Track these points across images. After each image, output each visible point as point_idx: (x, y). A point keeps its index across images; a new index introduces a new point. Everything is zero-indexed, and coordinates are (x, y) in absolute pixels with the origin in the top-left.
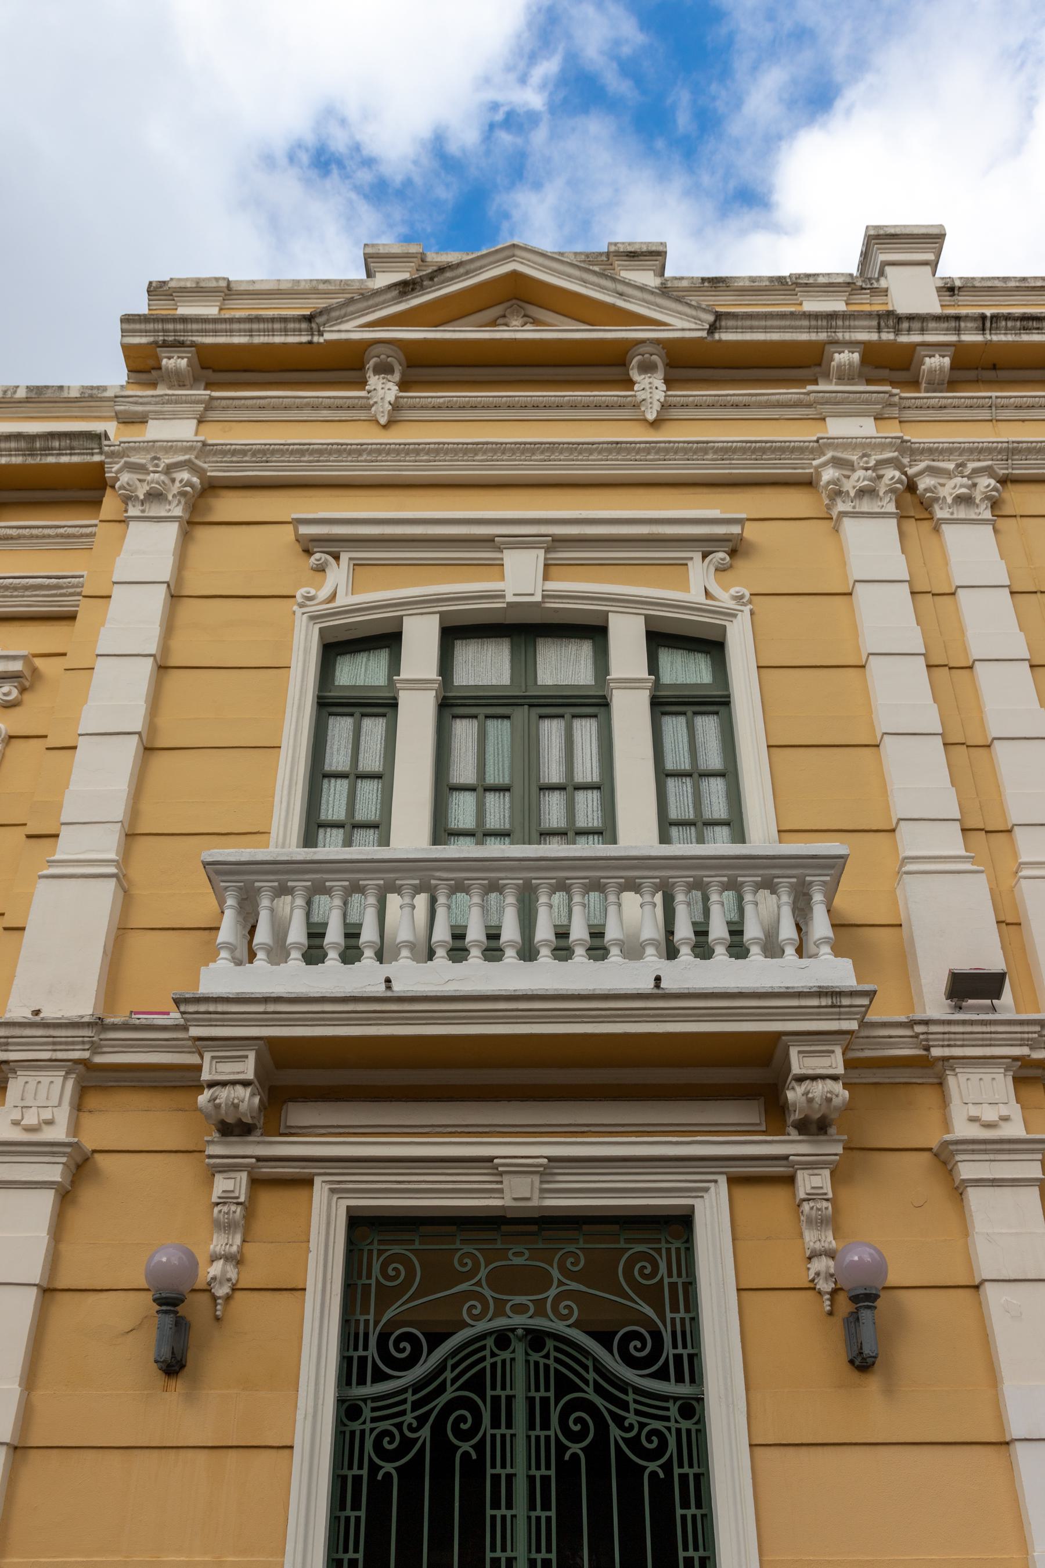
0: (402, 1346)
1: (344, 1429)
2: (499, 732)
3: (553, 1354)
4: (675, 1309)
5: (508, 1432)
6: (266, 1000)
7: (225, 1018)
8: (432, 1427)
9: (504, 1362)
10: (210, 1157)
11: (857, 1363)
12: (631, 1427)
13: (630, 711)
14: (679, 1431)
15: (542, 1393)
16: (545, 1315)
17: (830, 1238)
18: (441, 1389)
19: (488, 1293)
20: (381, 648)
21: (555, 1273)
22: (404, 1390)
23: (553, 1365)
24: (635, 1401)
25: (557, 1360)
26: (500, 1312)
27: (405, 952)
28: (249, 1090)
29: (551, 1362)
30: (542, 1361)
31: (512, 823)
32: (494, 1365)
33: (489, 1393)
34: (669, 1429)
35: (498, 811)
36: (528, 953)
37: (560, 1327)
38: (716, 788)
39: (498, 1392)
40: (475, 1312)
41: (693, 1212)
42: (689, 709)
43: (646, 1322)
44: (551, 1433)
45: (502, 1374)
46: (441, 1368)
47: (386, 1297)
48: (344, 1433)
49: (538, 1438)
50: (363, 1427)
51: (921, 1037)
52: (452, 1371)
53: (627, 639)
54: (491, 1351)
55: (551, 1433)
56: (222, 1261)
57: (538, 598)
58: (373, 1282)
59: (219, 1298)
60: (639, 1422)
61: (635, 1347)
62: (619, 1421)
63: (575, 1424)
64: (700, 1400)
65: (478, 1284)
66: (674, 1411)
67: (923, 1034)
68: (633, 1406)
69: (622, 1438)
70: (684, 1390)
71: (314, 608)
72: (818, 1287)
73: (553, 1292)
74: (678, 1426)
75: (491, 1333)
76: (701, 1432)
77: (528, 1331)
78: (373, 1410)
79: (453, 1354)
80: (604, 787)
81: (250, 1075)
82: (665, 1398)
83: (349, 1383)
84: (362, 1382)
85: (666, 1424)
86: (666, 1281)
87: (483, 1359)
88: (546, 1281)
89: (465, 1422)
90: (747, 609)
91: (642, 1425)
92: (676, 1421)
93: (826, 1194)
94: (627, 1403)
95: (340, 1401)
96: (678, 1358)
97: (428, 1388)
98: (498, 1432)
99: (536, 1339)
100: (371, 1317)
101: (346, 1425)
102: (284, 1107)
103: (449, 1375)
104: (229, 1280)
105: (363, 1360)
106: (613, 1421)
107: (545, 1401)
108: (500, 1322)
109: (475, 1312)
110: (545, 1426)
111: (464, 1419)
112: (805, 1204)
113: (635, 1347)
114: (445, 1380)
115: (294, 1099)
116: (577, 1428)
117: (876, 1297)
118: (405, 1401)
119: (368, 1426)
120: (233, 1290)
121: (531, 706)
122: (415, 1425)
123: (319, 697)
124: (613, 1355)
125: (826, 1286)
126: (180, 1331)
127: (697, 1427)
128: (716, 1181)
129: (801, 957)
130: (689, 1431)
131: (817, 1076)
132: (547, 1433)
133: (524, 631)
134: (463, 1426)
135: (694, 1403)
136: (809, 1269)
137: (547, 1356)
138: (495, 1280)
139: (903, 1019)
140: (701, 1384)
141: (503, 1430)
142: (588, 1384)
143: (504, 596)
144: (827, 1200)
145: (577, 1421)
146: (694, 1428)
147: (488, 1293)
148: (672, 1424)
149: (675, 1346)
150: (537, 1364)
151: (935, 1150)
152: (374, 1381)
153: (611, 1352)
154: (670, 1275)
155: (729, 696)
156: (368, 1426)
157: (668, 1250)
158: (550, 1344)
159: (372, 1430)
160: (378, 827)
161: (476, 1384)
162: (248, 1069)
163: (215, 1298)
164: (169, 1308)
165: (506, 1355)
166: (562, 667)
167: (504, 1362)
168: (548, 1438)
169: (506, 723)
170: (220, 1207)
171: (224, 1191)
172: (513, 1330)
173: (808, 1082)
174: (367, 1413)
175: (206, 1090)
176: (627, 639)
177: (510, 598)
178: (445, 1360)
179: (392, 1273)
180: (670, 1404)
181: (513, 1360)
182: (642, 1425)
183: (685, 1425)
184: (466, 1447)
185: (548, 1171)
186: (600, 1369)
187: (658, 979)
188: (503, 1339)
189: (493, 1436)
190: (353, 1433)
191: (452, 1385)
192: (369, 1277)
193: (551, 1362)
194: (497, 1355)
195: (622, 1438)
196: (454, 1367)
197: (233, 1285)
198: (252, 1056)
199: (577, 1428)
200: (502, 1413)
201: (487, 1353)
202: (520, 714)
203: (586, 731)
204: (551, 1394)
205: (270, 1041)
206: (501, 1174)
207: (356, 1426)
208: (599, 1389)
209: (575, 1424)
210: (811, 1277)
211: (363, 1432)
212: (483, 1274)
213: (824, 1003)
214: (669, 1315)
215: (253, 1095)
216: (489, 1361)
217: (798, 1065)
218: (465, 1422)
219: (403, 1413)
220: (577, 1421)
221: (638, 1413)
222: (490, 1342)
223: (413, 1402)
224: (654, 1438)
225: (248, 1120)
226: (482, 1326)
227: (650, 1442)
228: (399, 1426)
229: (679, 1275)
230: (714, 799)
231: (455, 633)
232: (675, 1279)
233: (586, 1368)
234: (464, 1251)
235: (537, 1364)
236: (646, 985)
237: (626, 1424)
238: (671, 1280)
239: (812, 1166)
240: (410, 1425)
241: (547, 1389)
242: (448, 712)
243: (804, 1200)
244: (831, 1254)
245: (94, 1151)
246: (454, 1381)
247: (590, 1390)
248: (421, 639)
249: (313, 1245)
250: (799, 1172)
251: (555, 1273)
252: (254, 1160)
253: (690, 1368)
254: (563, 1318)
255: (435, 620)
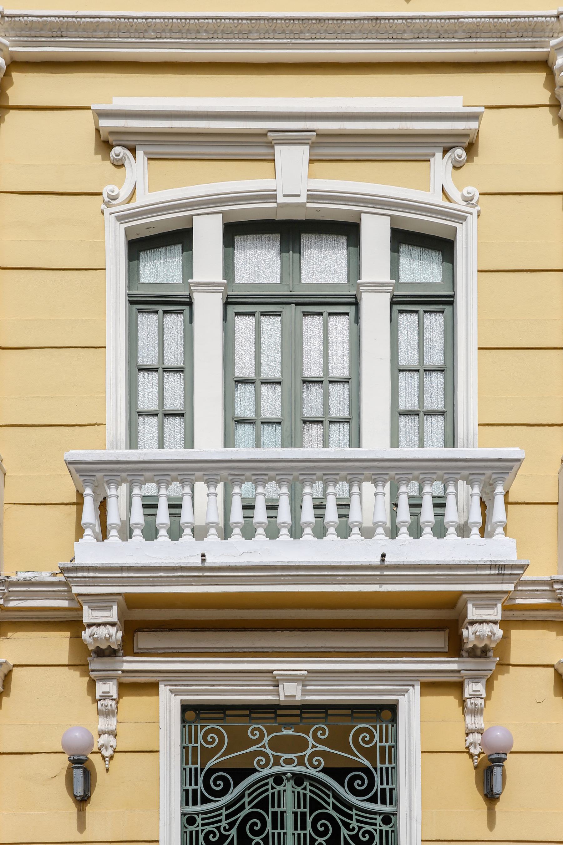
0: (218, 783)
1: (185, 830)
2: (272, 327)
3: (308, 787)
4: (383, 761)
5: (282, 832)
6: (122, 569)
7: (94, 582)
8: (238, 829)
9: (279, 792)
10: (93, 671)
11: (489, 796)
12: (354, 829)
13: (375, 307)
14: (381, 831)
15: (302, 810)
16: (304, 765)
17: (482, 722)
18: (242, 807)
19: (269, 751)
20: (175, 244)
21: (310, 740)
22: (221, 808)
23: (308, 794)
24: (357, 815)
25: (311, 791)
26: (277, 762)
27: (213, 531)
28: (115, 628)
29: (307, 792)
30: (302, 792)
31: (282, 414)
32: (273, 794)
33: (271, 810)
34: (376, 830)
35: (272, 402)
36: (296, 532)
37: (313, 772)
38: (436, 381)
39: (276, 809)
40: (261, 763)
41: (398, 703)
42: (421, 308)
43: (366, 770)
44: (307, 832)
45: (278, 798)
46: (242, 796)
47: (208, 754)
48: (186, 832)
49: (299, 834)
50: (197, 829)
51: (558, 591)
52: (248, 798)
53: (375, 233)
54: (272, 785)
55: (307, 832)
56: (106, 735)
57: (303, 199)
58: (198, 745)
59: (107, 757)
60: (358, 826)
61: (358, 784)
62: (347, 825)
63: (321, 827)
64: (395, 814)
65: (264, 746)
66: (379, 819)
67: (559, 589)
68: (355, 817)
69: (348, 835)
70: (386, 808)
71: (121, 208)
72: (471, 751)
73: (309, 751)
74: (381, 828)
75: (271, 776)
76: (395, 832)
77: (294, 774)
78: (203, 819)
79: (249, 788)
80: (352, 381)
81: (115, 619)
82: (375, 813)
83: (187, 804)
84: (195, 803)
85: (374, 827)
86: (379, 745)
87: (267, 790)
88: (304, 745)
89: (257, 826)
90: (474, 211)
91: (360, 828)
92: (380, 826)
93: (481, 695)
94: (352, 815)
95: (183, 815)
96: (383, 791)
97: (235, 807)
98: (276, 832)
99: (299, 779)
100: (199, 766)
101: (186, 828)
102: (136, 635)
103: (246, 799)
104: (112, 747)
105: (195, 792)
106: (343, 825)
107: (303, 814)
108: (277, 769)
109: (261, 763)
110: (304, 827)
111: (256, 824)
112: (468, 700)
113: (358, 784)
114: (244, 803)
115: (141, 630)
116: (322, 829)
117: (502, 760)
118: (221, 814)
119: (200, 828)
120: (115, 752)
121: (297, 304)
122: (227, 827)
123: (129, 296)
124: (344, 787)
125: (475, 751)
126: (82, 776)
127: (393, 829)
128: (413, 686)
129: (482, 536)
130: (387, 832)
131: (482, 623)
132: (305, 832)
133: (290, 232)
134: (256, 828)
135: (392, 816)
136: (466, 740)
137: (305, 789)
138: (273, 744)
139: (547, 578)
140: (397, 804)
141: (279, 830)
142: (329, 805)
143: (275, 197)
144: (482, 698)
145: (322, 825)
146: (390, 830)
147: (269, 751)
148: (377, 827)
149: (382, 784)
150: (299, 793)
151: (556, 667)
152: (202, 803)
153: (343, 786)
154: (381, 741)
155: (453, 296)
156: (200, 828)
157: (381, 727)
158: (306, 783)
159: (202, 830)
160: (183, 416)
161: (263, 804)
162: (113, 615)
163: (104, 758)
164: (79, 765)
165: (280, 788)
166: (323, 264)
167: (279, 792)
168: (305, 835)
169: (277, 320)
170: (102, 702)
171: (103, 693)
172: (285, 774)
173: (477, 624)
174: (199, 821)
175: (87, 630)
176: (375, 233)
177: (281, 200)
178: (245, 791)
179: (210, 740)
180: (377, 817)
181: (284, 791)
182: (360, 828)
183: (385, 828)
184: (257, 839)
185: (308, 678)
186: (336, 796)
187: (383, 555)
188: (278, 779)
189: (273, 834)
190: (191, 832)
191: (248, 805)
192: (196, 742)
193: (307, 792)
194: (275, 788)
195: (348, 835)
196: (249, 795)
197: (115, 749)
198: (115, 608)
199: (322, 829)
200: (278, 821)
201: (269, 787)
202: (287, 311)
203: (339, 326)
204: (307, 810)
205: (127, 597)
206: (278, 681)
207: (193, 828)
208: (335, 808)
209: (321, 827)
210: (467, 746)
211: (197, 832)
212: (266, 740)
213: (493, 572)
214: (379, 765)
215: (117, 631)
216: (271, 791)
217: (472, 613)
218: (257, 826)
219: (220, 821)
220: (322, 825)
221: (358, 821)
222: (271, 781)
223: (226, 815)
224: (367, 835)
225: (115, 647)
226: (266, 772)
227: (365, 837)
228: (218, 828)
229: (387, 742)
230: (434, 390)
231: (236, 231)
232: (384, 744)
233: (328, 796)
234: (254, 729)
235: (299, 793)
236: (376, 560)
237: (351, 827)
238: (381, 745)
239: (475, 679)
240: (224, 828)
241: (305, 807)
242: (232, 309)
243: (468, 698)
244: (480, 732)
245: (15, 666)
246: (249, 803)
247: (330, 808)
248: (208, 233)
249: (161, 724)
250: (466, 680)
251: (310, 740)
252: (120, 672)
253: (389, 796)
254: (315, 767)
255: (219, 219)
